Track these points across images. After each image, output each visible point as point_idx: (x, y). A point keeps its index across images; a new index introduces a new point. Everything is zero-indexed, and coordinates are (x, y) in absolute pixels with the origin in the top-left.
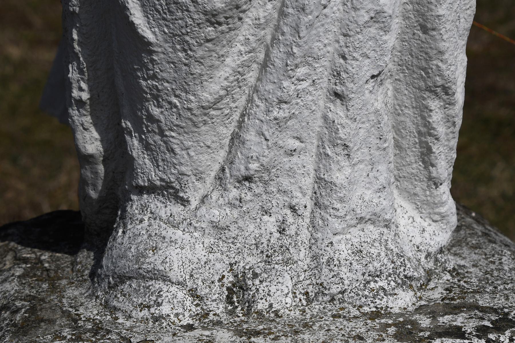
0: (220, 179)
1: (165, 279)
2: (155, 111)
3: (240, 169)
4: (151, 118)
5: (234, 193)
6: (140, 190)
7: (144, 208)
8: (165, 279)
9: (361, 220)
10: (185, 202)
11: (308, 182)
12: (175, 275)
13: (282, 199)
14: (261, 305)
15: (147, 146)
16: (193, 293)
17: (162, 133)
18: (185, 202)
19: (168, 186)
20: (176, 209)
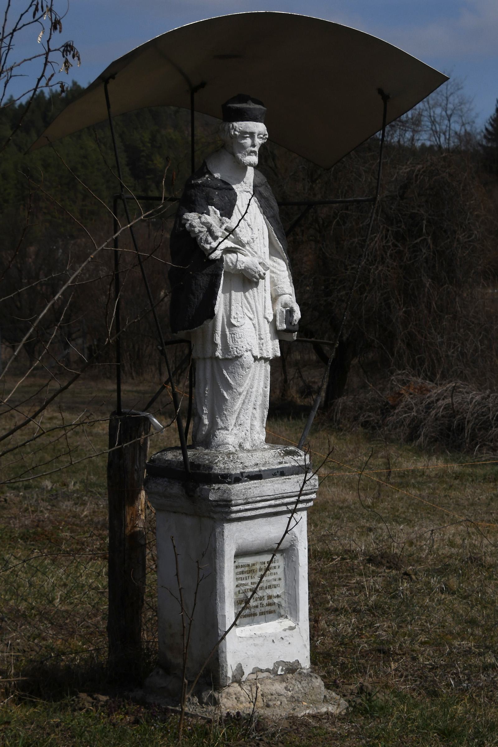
0: (235, 425)
1: (228, 444)
2: (225, 412)
3: (239, 423)
4: (224, 414)
5: (238, 428)
6: (219, 429)
7: (220, 433)
8: (228, 444)
10: (228, 430)
11: (249, 425)
12: (230, 443)
13: (245, 429)
14: (245, 448)
15: (222, 420)
16: (234, 447)
17: (226, 417)
18: (228, 430)
19: (225, 427)
20: (227, 432)
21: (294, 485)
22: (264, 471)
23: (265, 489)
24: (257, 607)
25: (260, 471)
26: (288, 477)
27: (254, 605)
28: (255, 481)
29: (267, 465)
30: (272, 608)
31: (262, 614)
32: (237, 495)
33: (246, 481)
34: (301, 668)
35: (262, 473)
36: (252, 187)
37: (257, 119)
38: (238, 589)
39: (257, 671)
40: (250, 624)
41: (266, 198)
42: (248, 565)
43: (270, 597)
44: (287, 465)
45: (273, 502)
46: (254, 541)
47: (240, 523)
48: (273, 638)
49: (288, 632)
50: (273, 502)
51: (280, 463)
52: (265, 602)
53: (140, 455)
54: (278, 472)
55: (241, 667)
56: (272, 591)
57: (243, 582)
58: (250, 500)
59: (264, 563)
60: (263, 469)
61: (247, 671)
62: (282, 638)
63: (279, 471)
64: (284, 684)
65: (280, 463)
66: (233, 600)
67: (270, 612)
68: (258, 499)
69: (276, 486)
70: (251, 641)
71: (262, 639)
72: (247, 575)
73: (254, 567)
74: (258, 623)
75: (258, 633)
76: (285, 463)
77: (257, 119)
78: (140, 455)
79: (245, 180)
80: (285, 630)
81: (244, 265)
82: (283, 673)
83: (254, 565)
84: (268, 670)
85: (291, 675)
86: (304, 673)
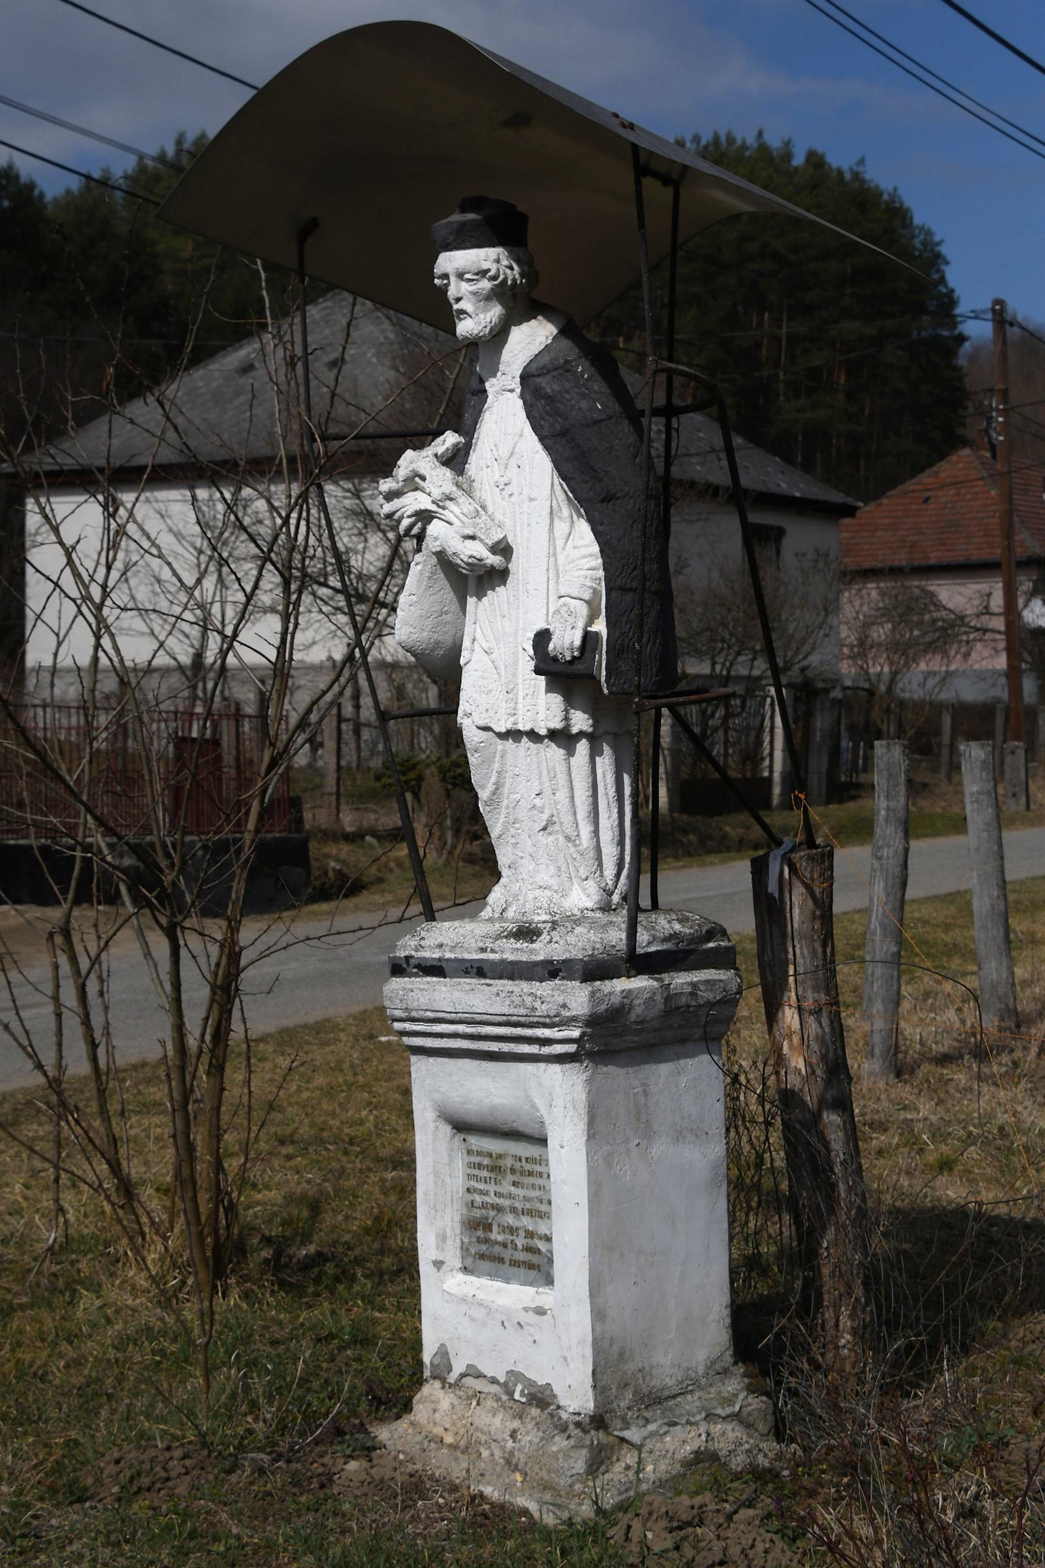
9: (541, 887)
21: (490, 999)
22: (448, 960)
23: (437, 996)
24: (505, 1245)
25: (440, 960)
26: (488, 981)
27: (500, 1238)
28: (434, 979)
29: (458, 950)
30: (534, 1259)
31: (515, 1263)
32: (390, 999)
33: (416, 975)
34: (559, 1407)
35: (444, 965)
36: (518, 379)
37: (448, 244)
38: (470, 1197)
39: (473, 1372)
40: (492, 1276)
41: (549, 397)
42: (491, 1155)
43: (530, 1235)
44: (492, 956)
45: (461, 1028)
46: (465, 1103)
47: (431, 1060)
48: (504, 1318)
49: (531, 1317)
50: (461, 1028)
51: (483, 950)
52: (520, 1242)
53: (771, 934)
54: (472, 967)
55: (447, 1353)
56: (536, 1223)
57: (481, 1186)
58: (414, 1014)
59: (520, 1160)
60: (448, 955)
61: (458, 1368)
62: (519, 1323)
63: (475, 965)
64: (516, 1424)
65: (483, 950)
66: (457, 1218)
67: (531, 1266)
68: (429, 1014)
69: (456, 994)
70: (464, 1308)
71: (483, 1311)
72: (485, 1173)
73: (501, 1163)
74: (507, 1281)
75: (481, 1296)
76: (493, 951)
77: (448, 244)
78: (771, 934)
79: (501, 367)
80: (526, 1309)
81: (438, 543)
82: (524, 1400)
83: (500, 1156)
84: (494, 1381)
85: (539, 1411)
86: (560, 1418)
